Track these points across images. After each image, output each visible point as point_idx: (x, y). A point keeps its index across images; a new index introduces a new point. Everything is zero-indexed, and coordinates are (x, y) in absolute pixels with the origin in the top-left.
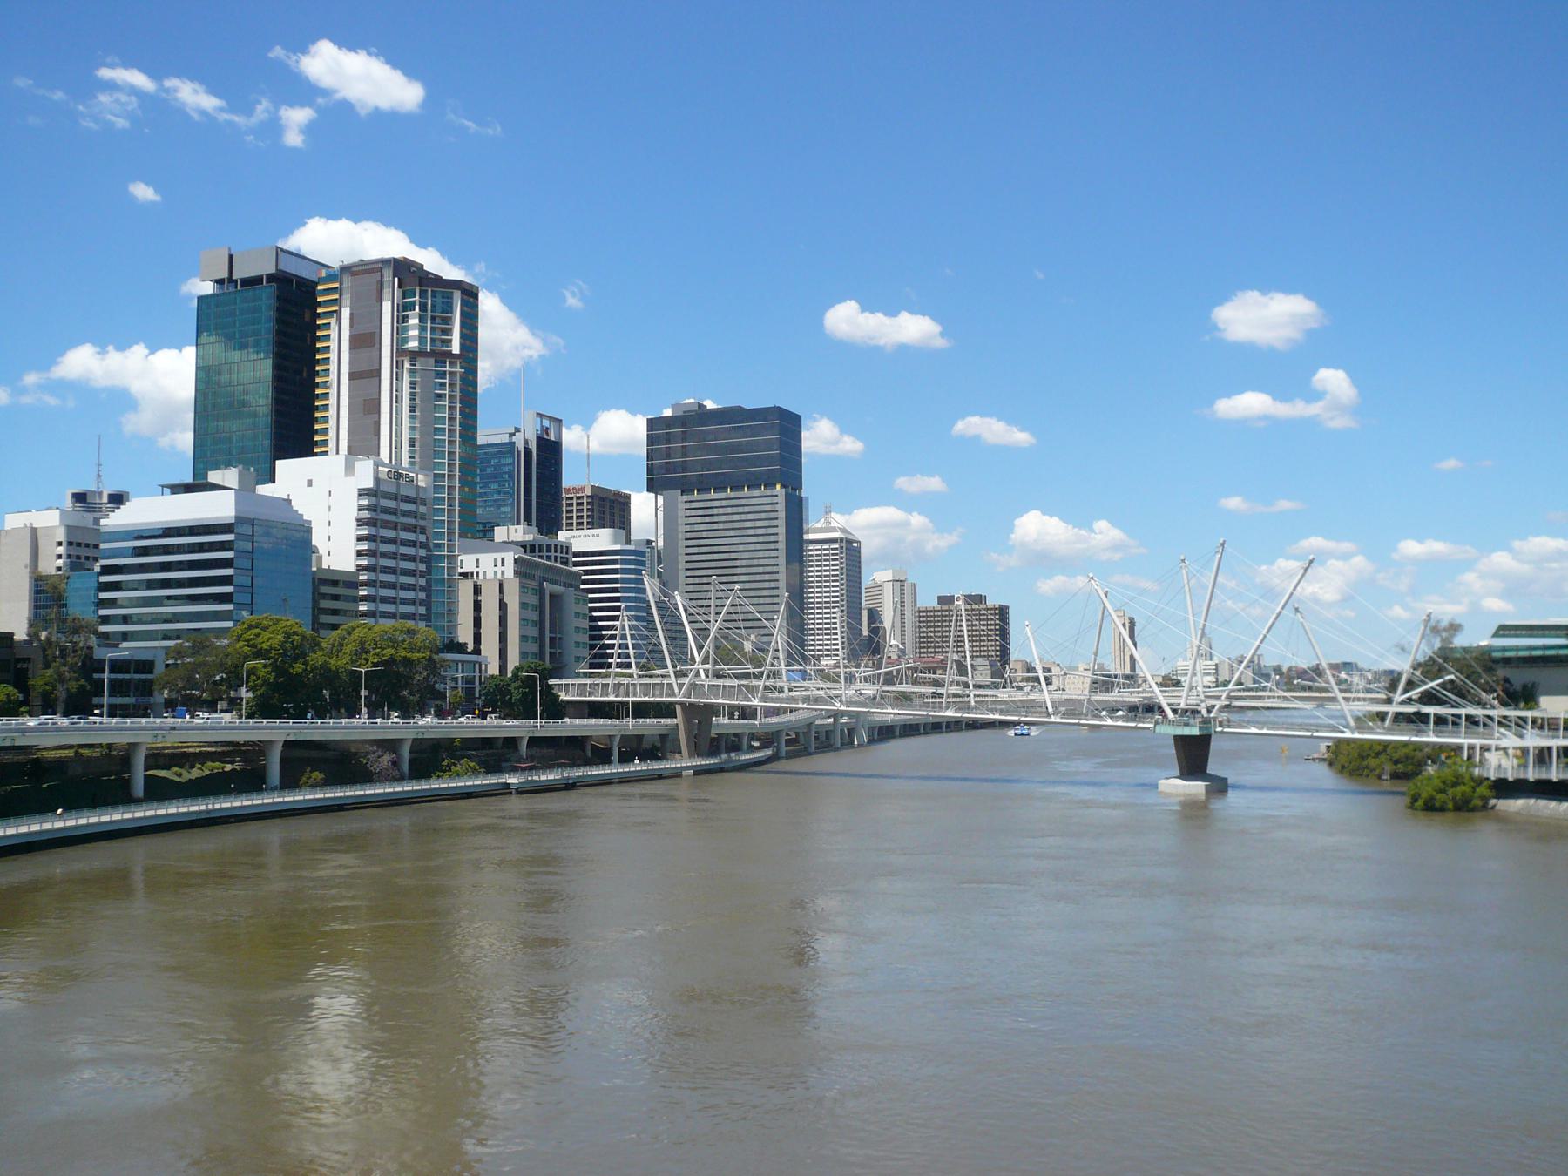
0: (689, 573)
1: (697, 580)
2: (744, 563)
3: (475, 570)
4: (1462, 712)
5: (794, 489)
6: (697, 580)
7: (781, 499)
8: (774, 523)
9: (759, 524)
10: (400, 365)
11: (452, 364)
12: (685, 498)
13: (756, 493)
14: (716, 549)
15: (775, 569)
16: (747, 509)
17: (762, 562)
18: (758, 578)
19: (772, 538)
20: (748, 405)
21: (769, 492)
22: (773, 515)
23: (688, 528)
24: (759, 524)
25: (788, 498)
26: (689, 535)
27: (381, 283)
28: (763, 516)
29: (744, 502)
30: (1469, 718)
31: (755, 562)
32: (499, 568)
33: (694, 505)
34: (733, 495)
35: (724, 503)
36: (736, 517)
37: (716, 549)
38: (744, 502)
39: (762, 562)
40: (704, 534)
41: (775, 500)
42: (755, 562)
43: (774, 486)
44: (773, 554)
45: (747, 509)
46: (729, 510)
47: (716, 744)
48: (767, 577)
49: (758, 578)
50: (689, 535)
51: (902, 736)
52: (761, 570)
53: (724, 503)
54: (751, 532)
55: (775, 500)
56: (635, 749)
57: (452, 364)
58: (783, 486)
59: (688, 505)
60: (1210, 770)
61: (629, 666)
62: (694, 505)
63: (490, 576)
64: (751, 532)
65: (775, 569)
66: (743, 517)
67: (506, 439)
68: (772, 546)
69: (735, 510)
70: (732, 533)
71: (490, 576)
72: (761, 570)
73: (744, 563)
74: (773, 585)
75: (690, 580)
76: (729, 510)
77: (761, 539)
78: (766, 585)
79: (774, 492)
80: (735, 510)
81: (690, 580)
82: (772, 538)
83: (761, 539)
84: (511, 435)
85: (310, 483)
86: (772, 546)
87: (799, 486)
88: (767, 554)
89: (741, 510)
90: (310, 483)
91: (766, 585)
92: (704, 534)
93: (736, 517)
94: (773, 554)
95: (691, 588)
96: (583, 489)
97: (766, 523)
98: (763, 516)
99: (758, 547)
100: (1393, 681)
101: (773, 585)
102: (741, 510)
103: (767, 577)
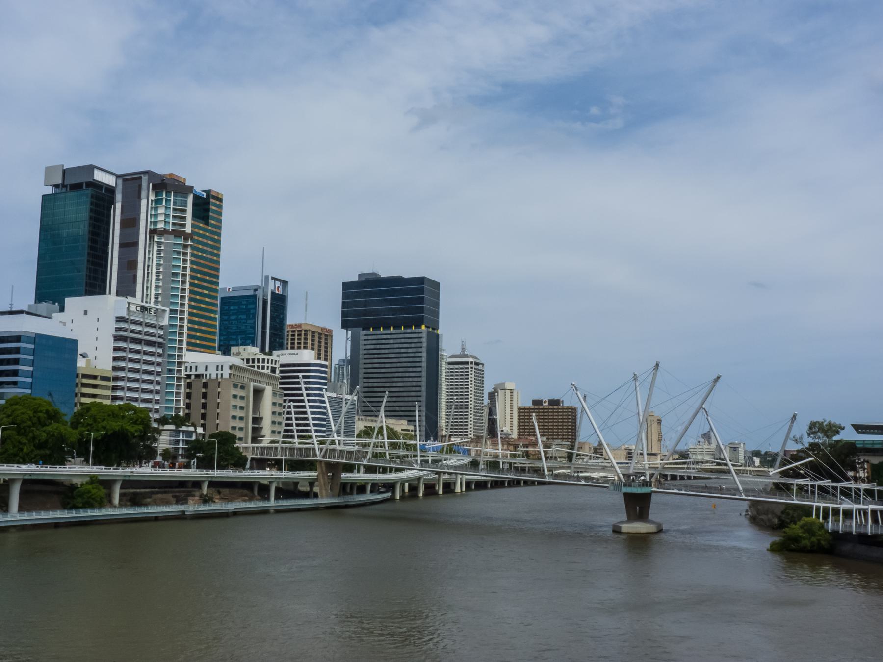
0: (365, 380)
1: (370, 385)
2: (400, 375)
3: (204, 372)
4: (840, 485)
6: (370, 385)
7: (424, 335)
8: (420, 350)
9: (410, 350)
10: (152, 238)
11: (186, 239)
12: (365, 333)
13: (409, 331)
14: (383, 365)
15: (419, 379)
16: (403, 341)
18: (409, 384)
19: (418, 360)
20: (406, 275)
21: (417, 330)
22: (419, 345)
23: (366, 352)
24: (410, 350)
26: (366, 356)
27: (140, 187)
28: (413, 345)
29: (401, 336)
30: (821, 488)
31: (407, 374)
32: (220, 372)
33: (370, 337)
35: (389, 337)
36: (396, 346)
37: (383, 365)
38: (401, 336)
40: (376, 356)
41: (420, 335)
42: (407, 374)
44: (419, 369)
45: (403, 341)
46: (392, 341)
47: (346, 488)
48: (414, 384)
49: (409, 384)
50: (366, 356)
51: (492, 487)
52: (410, 379)
53: (389, 337)
54: (405, 355)
55: (420, 335)
56: (288, 491)
57: (186, 239)
58: (427, 327)
59: (366, 338)
60: (650, 517)
61: (292, 437)
62: (370, 337)
63: (214, 377)
64: (405, 355)
65: (419, 379)
66: (401, 346)
67: (251, 293)
68: (418, 364)
69: (396, 341)
70: (393, 355)
71: (214, 377)
72: (410, 379)
73: (400, 375)
74: (418, 389)
75: (366, 385)
76: (392, 341)
77: (411, 360)
78: (414, 389)
79: (420, 330)
80: (396, 341)
81: (366, 385)
82: (418, 360)
83: (411, 360)
84: (256, 290)
85: (86, 313)
86: (418, 364)
87: (436, 327)
88: (414, 369)
89: (399, 341)
90: (86, 313)
91: (414, 389)
92: (376, 356)
93: (396, 346)
94: (419, 369)
95: (366, 390)
97: (414, 350)
98: (413, 345)
99: (409, 365)
100: (768, 460)
101: (418, 389)
102: (399, 341)
103: (414, 384)
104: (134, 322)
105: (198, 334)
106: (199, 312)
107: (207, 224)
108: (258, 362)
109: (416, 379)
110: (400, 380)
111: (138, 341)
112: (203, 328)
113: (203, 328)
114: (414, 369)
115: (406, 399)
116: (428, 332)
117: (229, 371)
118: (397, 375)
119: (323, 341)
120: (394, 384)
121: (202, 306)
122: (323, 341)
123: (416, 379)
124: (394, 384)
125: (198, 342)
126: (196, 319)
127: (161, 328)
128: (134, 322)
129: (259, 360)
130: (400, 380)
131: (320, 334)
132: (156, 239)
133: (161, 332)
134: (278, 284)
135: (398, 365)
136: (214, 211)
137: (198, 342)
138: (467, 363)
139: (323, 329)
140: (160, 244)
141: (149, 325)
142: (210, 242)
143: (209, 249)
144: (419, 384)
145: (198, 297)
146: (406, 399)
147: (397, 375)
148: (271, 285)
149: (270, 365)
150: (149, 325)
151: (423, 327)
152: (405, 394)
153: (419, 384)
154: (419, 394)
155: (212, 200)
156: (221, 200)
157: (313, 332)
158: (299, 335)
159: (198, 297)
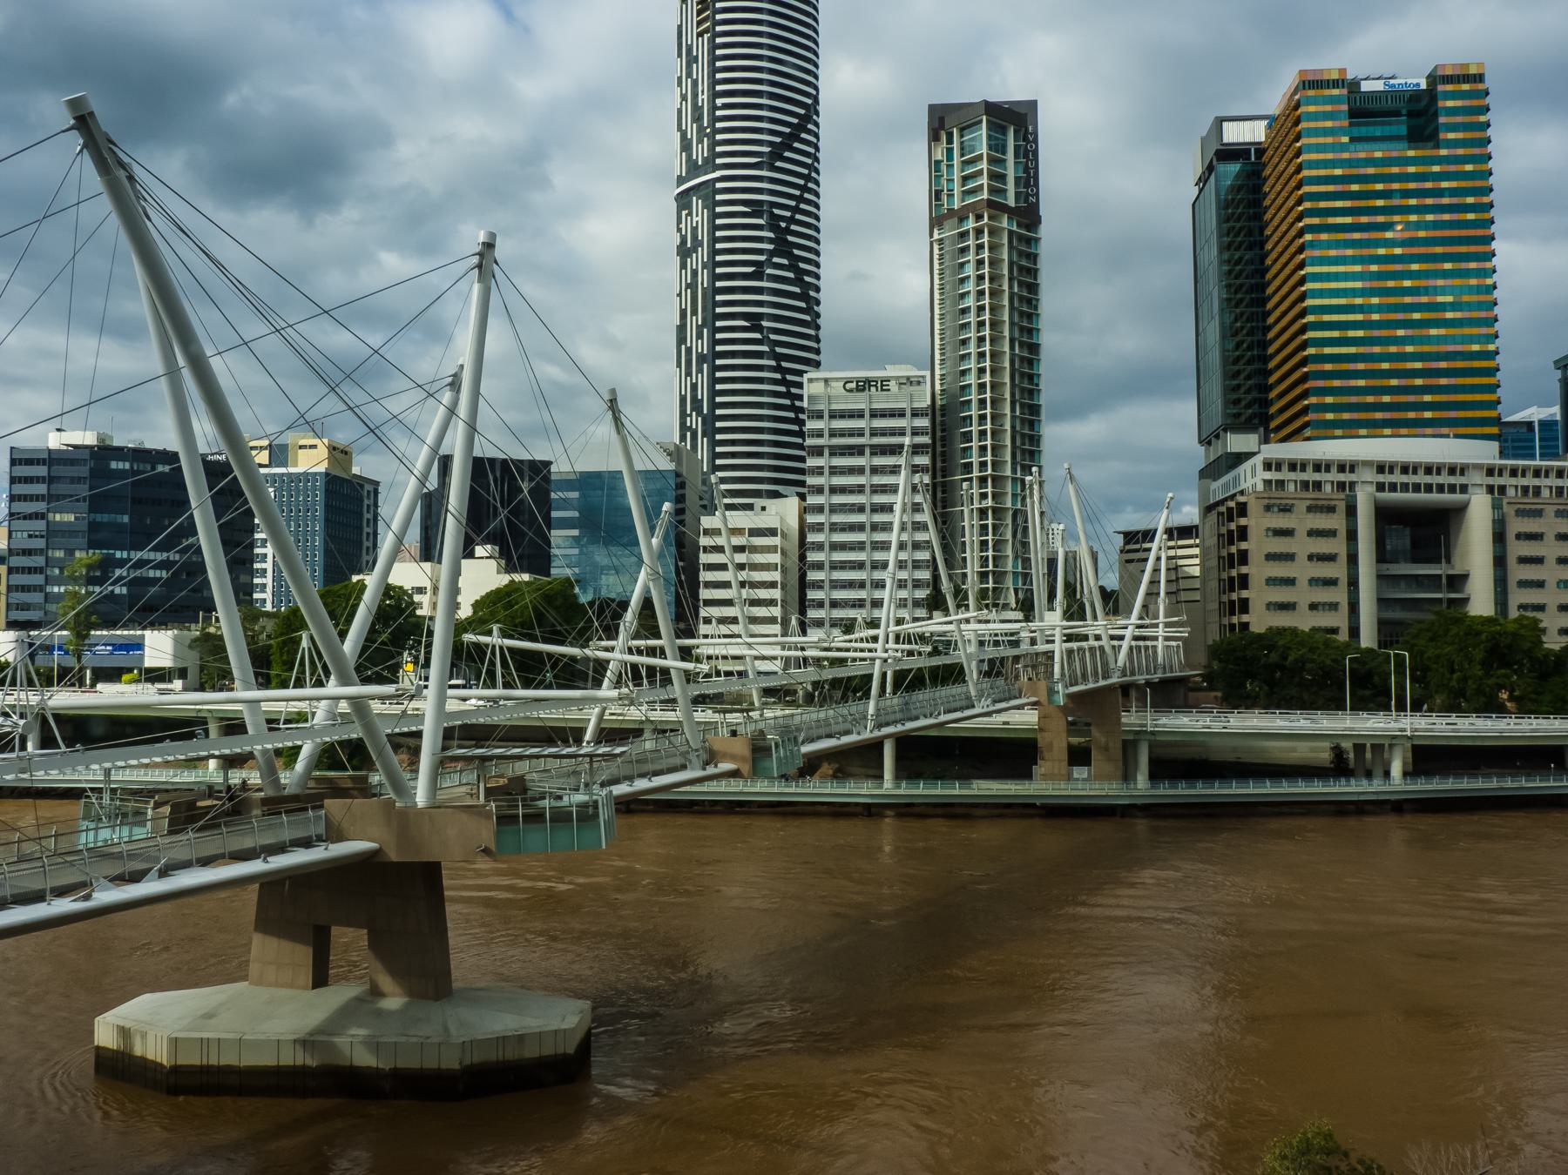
11: (979, 217)
104: (834, 415)
105: (1427, 398)
106: (1426, 349)
107: (1437, 146)
111: (858, 451)
112: (1443, 381)
113: (1443, 381)
117: (1268, 476)
121: (1433, 332)
125: (1428, 415)
126: (1418, 365)
127: (916, 414)
128: (834, 415)
132: (936, 236)
133: (924, 422)
137: (1428, 415)
140: (941, 241)
141: (874, 414)
142: (1445, 185)
143: (1446, 201)
145: (1416, 316)
150: (874, 414)
155: (1441, 88)
156: (1479, 78)
159: (1416, 316)
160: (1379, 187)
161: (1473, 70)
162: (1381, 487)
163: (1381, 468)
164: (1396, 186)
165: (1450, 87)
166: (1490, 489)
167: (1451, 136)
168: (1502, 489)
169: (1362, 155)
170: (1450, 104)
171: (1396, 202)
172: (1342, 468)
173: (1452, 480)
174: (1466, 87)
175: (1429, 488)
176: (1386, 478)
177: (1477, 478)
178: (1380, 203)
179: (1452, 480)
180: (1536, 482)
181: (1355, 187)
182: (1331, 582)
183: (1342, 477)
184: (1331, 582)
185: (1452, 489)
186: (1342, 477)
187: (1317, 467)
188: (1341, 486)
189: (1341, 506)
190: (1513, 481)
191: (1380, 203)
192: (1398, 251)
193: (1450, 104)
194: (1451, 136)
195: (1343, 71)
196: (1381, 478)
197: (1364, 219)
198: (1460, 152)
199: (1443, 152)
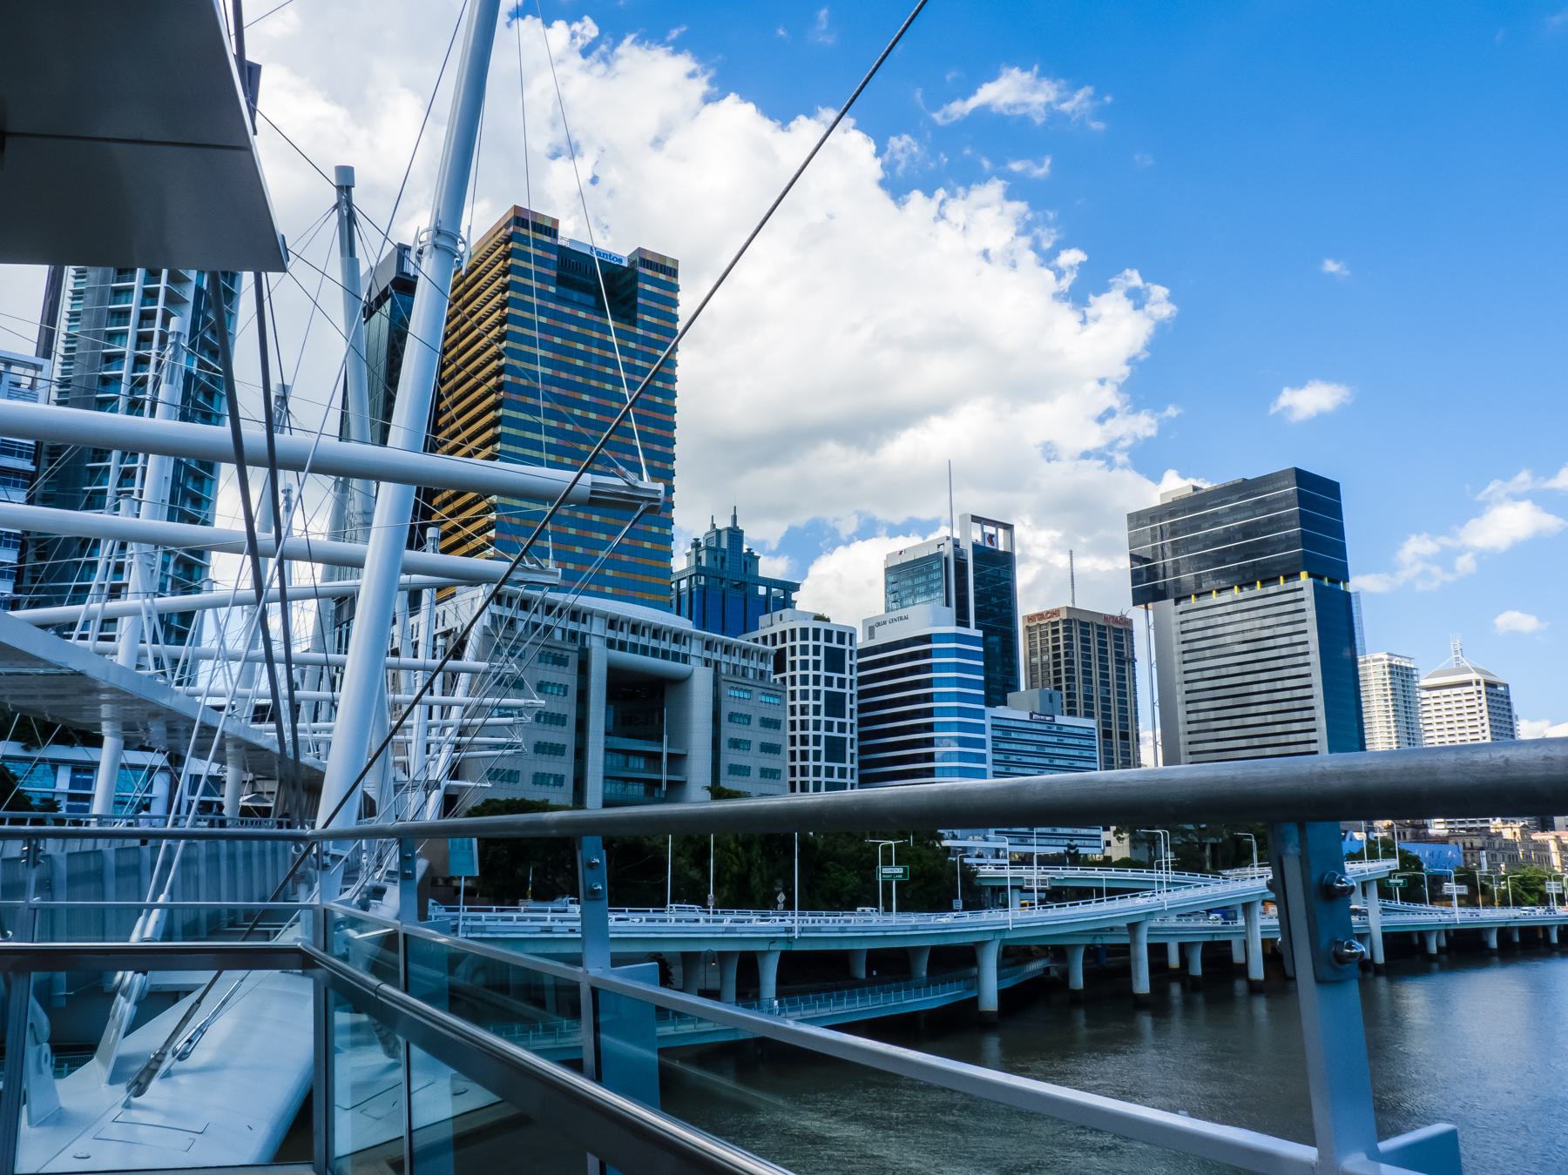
2: (1263, 687)
5: (1335, 581)
7: (1308, 593)
9: (1280, 630)
13: (1272, 589)
15: (1307, 692)
17: (1288, 683)
18: (1285, 706)
19: (1300, 649)
21: (1290, 585)
22: (1298, 617)
25: (1319, 592)
26: (1187, 657)
31: (1279, 685)
34: (1241, 596)
35: (1230, 608)
39: (1288, 683)
41: (1299, 595)
42: (1279, 685)
43: (1296, 576)
48: (1297, 704)
49: (1285, 706)
52: (1287, 695)
53: (1230, 608)
55: (1299, 595)
58: (1310, 575)
65: (1307, 692)
68: (1301, 660)
72: (1287, 695)
73: (1263, 687)
74: (1306, 714)
78: (1297, 715)
79: (1298, 584)
82: (1300, 649)
86: (1301, 660)
88: (1294, 672)
91: (1297, 715)
96: (1056, 613)
97: (1289, 629)
101: (1306, 714)
103: (1297, 704)
107: (634, 323)
108: (793, 639)
109: (1299, 693)
110: (1263, 698)
114: (1294, 672)
115: (1283, 739)
116: (1318, 589)
118: (1255, 688)
119: (1110, 641)
120: (1253, 710)
122: (1110, 641)
123: (1299, 693)
124: (1253, 710)
129: (793, 631)
130: (1263, 698)
131: (1099, 627)
134: (990, 530)
135: (1258, 666)
136: (650, 296)
138: (1469, 684)
139: (1106, 617)
144: (1308, 703)
146: (1283, 739)
147: (1255, 688)
148: (976, 535)
149: (822, 643)
151: (1304, 574)
152: (1279, 728)
153: (1308, 703)
154: (1309, 725)
155: (641, 270)
156: (673, 272)
157: (1083, 624)
158: (1056, 632)
160: (580, 347)
161: (669, 264)
162: (611, 644)
163: (613, 623)
164: (595, 351)
165: (649, 272)
166: (707, 663)
167: (647, 318)
168: (717, 663)
169: (567, 310)
170: (648, 287)
171: (594, 366)
172: (575, 615)
173: (675, 648)
174: (662, 277)
175: (655, 652)
176: (621, 636)
177: (695, 649)
178: (580, 363)
179: (675, 648)
180: (744, 662)
181: (557, 340)
182: (557, 750)
183: (572, 626)
184: (557, 750)
185: (676, 657)
186: (572, 626)
187: (549, 609)
188: (573, 635)
189: (573, 659)
190: (726, 658)
191: (580, 363)
192: (592, 416)
193: (648, 287)
194: (647, 318)
195: (556, 222)
196: (610, 634)
197: (564, 375)
198: (654, 336)
199: (639, 331)
